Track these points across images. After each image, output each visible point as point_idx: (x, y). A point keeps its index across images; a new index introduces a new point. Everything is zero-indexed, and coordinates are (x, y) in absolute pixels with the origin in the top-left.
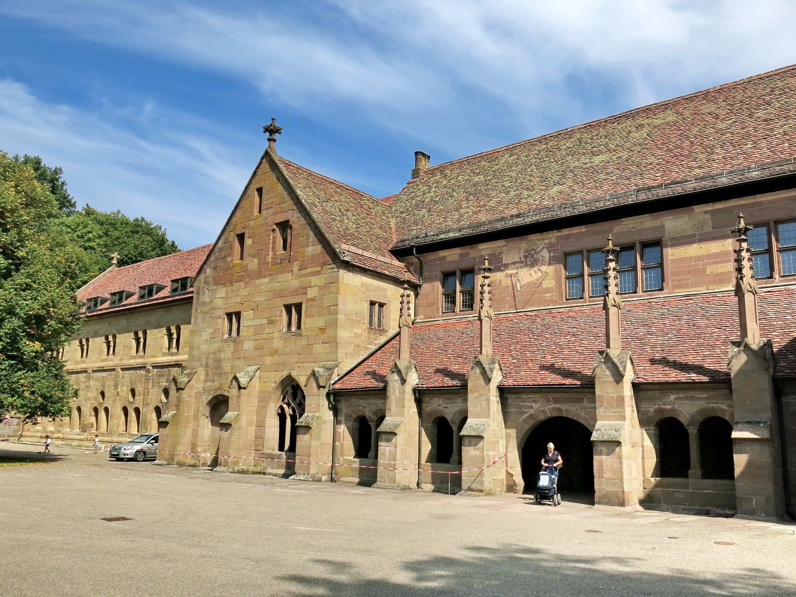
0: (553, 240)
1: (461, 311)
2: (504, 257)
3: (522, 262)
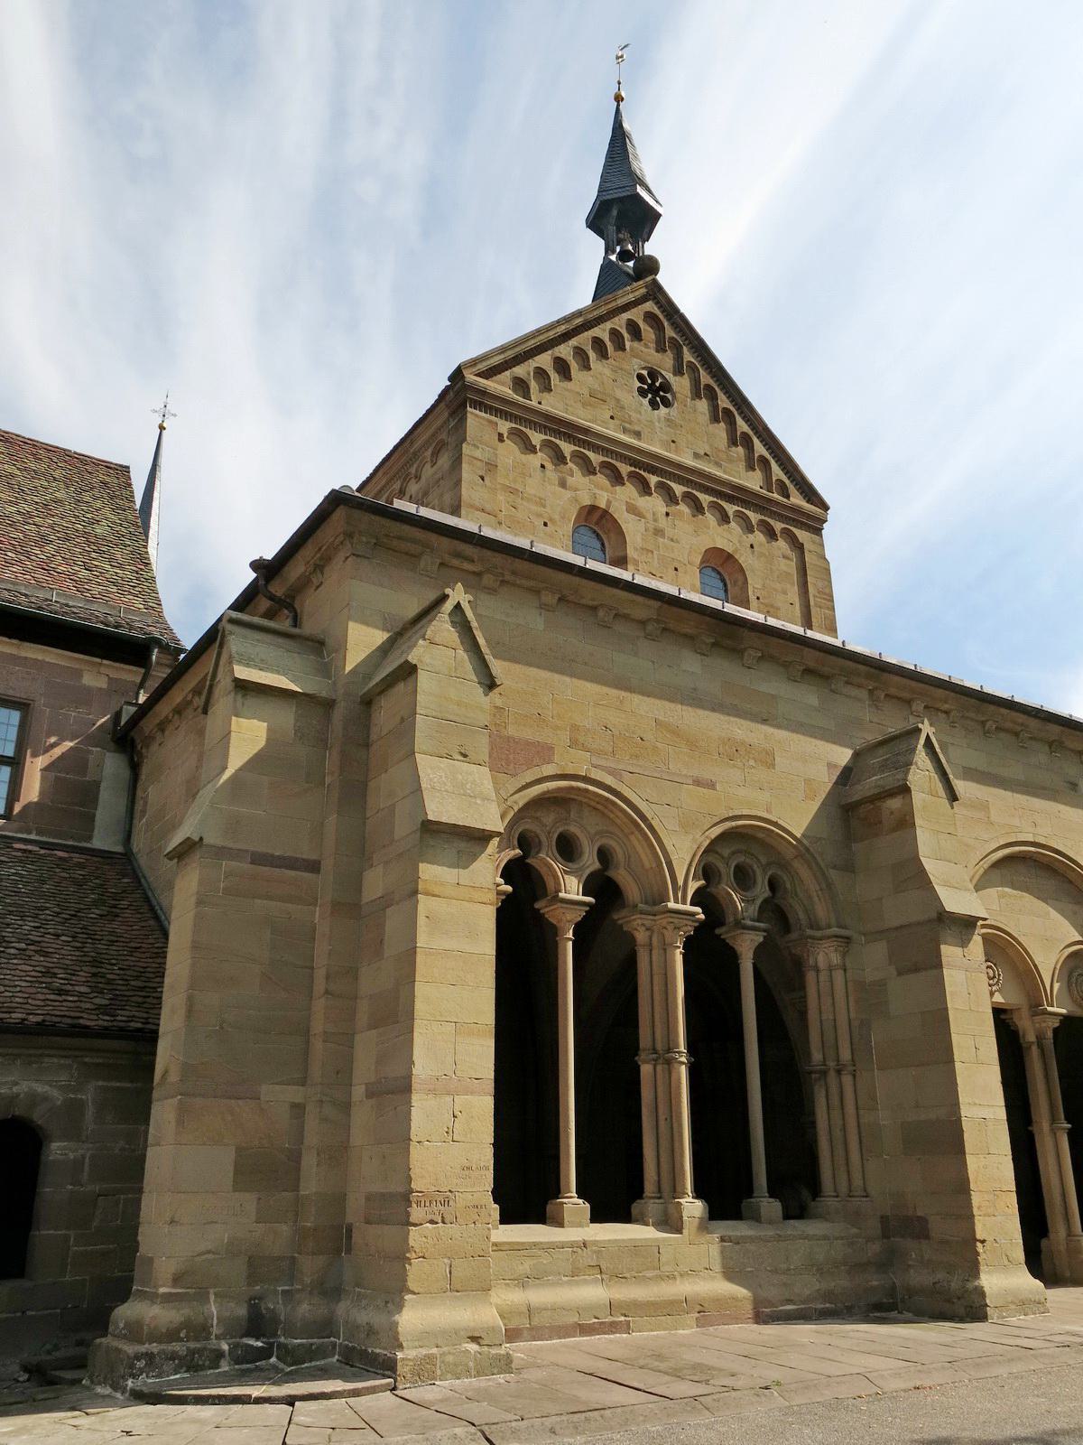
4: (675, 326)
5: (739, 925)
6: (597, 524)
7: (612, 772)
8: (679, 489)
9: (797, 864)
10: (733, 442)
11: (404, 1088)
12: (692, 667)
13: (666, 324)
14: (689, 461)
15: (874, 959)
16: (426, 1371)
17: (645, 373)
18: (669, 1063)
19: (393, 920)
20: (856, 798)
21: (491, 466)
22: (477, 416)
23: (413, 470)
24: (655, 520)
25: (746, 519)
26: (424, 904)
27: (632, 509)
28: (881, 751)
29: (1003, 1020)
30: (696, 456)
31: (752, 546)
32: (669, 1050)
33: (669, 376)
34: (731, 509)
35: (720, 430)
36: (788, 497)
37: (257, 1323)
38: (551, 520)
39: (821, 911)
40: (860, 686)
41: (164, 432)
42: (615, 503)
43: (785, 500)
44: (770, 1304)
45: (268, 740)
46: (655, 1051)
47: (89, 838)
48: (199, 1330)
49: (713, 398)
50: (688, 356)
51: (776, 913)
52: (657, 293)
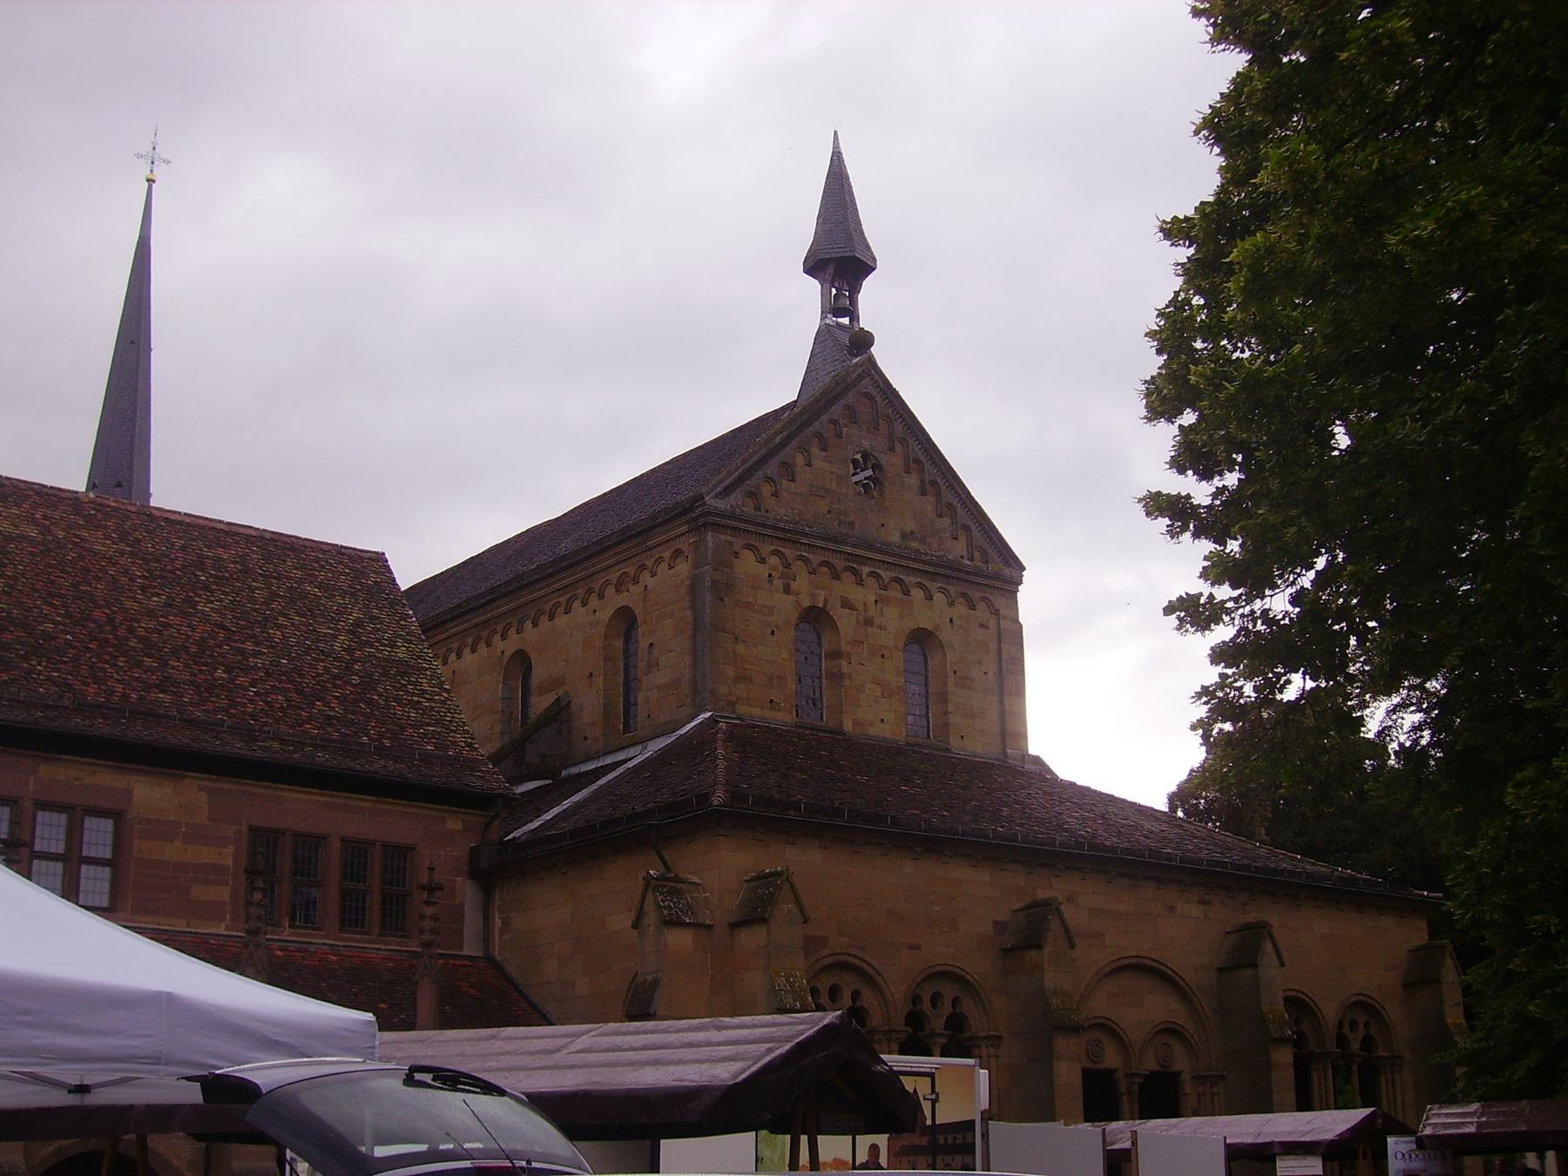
8: (886, 575)
17: (858, 456)
27: (847, 604)
31: (951, 620)
38: (777, 626)
47: (461, 948)
49: (922, 472)
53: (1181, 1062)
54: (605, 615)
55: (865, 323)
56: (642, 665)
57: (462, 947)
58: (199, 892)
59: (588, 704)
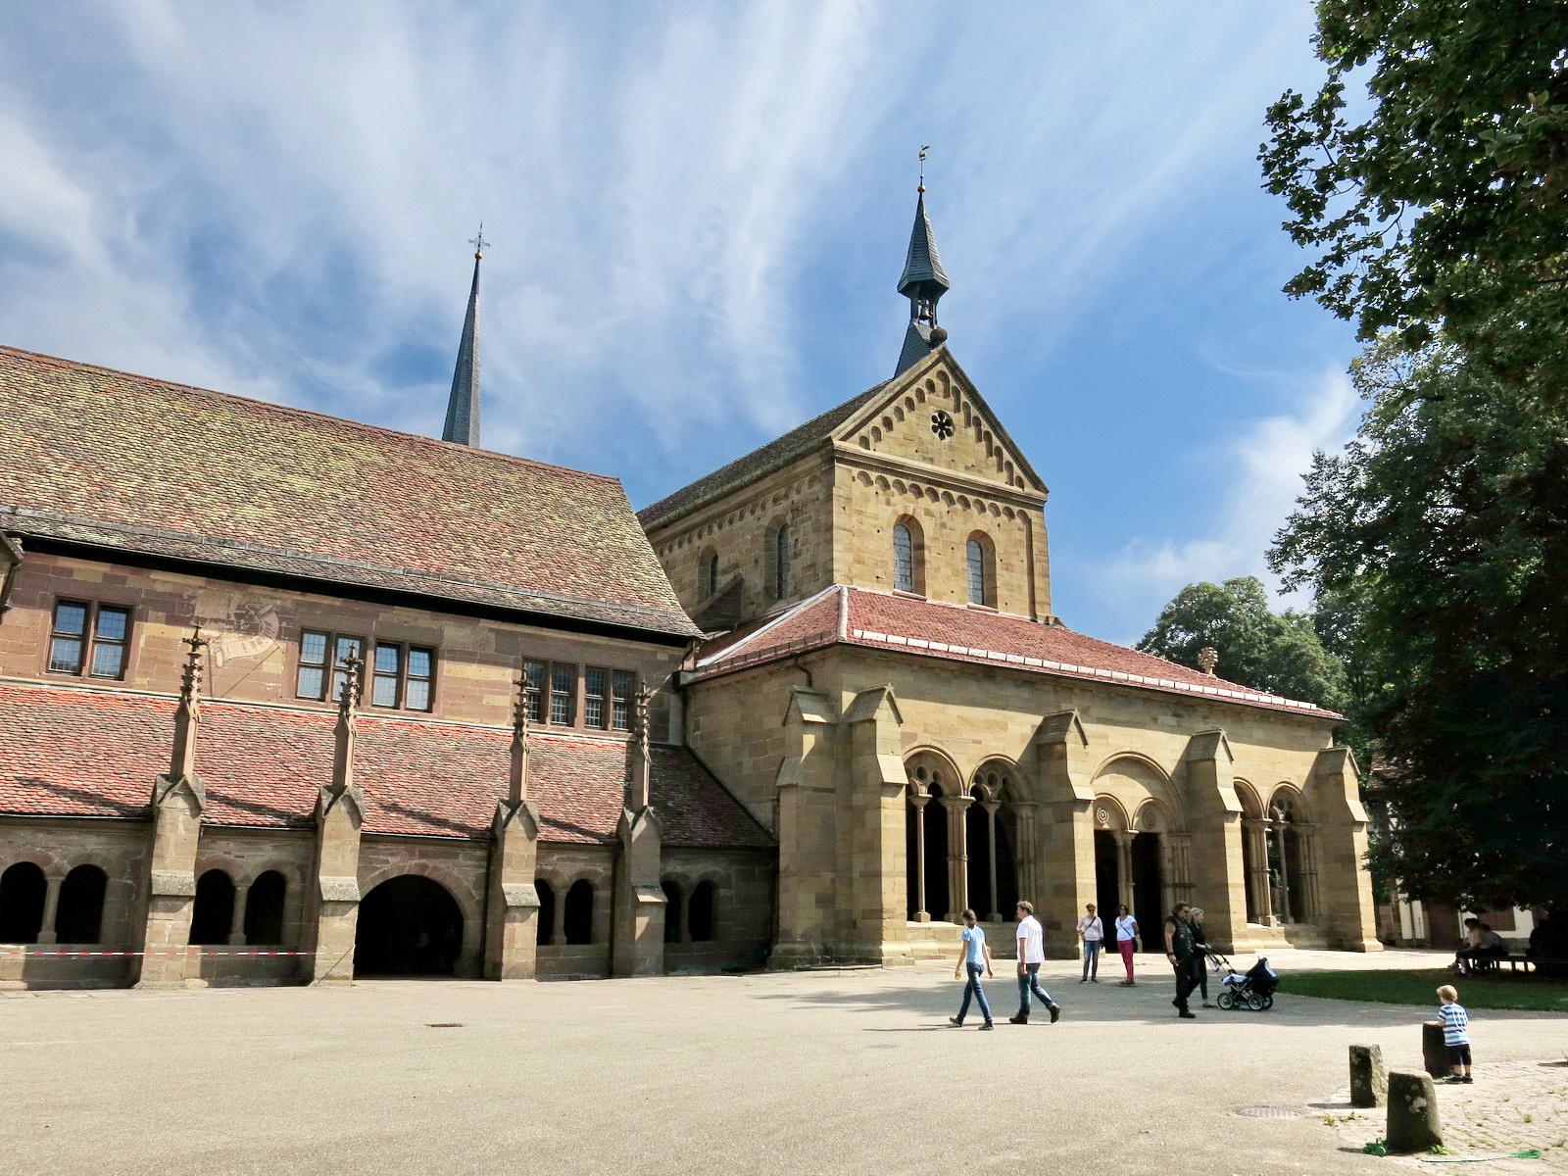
0: (288, 604)
1: (91, 676)
2: (198, 606)
3: (231, 623)
4: (956, 377)
5: (990, 802)
6: (907, 523)
7: (940, 742)
8: (955, 494)
9: (1015, 772)
10: (990, 454)
11: (878, 875)
12: (973, 688)
13: (950, 377)
14: (963, 475)
15: (1047, 815)
16: (890, 963)
17: (936, 414)
18: (960, 860)
19: (869, 816)
20: (1043, 742)
21: (849, 499)
22: (840, 467)
23: (796, 485)
24: (941, 518)
25: (996, 508)
26: (884, 812)
27: (928, 513)
28: (1056, 720)
29: (1103, 840)
30: (967, 468)
32: (960, 856)
33: (951, 414)
34: (987, 502)
35: (982, 446)
36: (1022, 487)
37: (826, 951)
39: (1025, 792)
40: (1048, 684)
41: (480, 261)
42: (918, 510)
43: (1021, 490)
44: (996, 952)
45: (816, 742)
46: (954, 855)
48: (811, 952)
49: (978, 424)
50: (964, 398)
51: (1006, 795)
52: (945, 356)
53: (1160, 827)
54: (766, 521)
55: (942, 324)
56: (790, 554)
57: (667, 739)
58: (488, 699)
59: (755, 581)
